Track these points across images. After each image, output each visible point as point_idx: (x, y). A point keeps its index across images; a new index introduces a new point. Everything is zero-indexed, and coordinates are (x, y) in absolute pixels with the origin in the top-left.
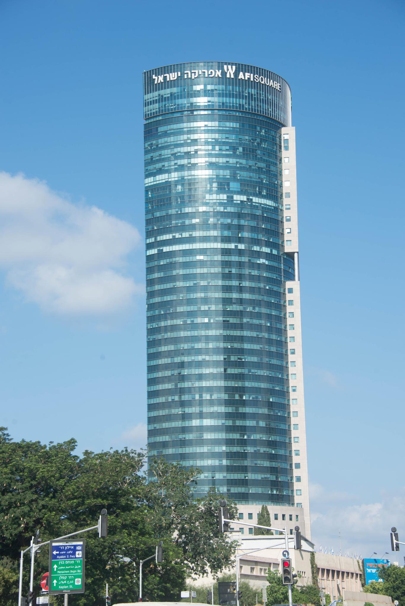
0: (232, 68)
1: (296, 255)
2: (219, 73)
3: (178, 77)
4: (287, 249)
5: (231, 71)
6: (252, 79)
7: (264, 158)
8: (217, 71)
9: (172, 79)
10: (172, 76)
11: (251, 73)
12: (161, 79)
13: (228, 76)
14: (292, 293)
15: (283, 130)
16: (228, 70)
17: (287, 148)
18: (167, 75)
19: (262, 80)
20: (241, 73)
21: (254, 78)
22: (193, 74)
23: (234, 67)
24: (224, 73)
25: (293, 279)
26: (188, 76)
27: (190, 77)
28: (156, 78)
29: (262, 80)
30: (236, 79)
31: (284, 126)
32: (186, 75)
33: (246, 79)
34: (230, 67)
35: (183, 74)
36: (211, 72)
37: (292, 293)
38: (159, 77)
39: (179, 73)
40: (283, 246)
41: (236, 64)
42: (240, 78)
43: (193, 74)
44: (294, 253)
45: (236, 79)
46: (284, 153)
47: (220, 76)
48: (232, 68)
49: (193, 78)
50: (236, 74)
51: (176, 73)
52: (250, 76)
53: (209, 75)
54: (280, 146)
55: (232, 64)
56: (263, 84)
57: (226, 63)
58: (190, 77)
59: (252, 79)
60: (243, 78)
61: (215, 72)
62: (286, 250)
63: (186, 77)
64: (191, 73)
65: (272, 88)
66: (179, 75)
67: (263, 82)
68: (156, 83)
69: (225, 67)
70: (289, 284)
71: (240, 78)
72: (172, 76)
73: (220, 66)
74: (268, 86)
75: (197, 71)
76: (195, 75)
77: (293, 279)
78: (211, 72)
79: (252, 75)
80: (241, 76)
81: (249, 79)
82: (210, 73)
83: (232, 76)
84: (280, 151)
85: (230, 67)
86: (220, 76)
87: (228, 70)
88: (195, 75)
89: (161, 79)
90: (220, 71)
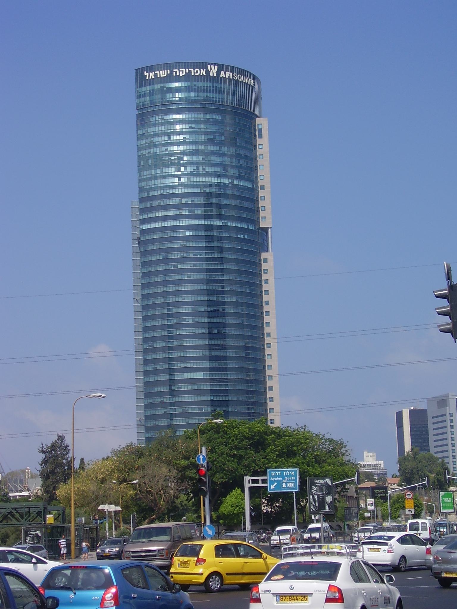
1: (269, 230)
2: (203, 72)
5: (213, 71)
6: (231, 77)
8: (202, 70)
9: (162, 76)
11: (231, 72)
12: (152, 75)
13: (211, 75)
14: (267, 262)
15: (258, 121)
16: (211, 69)
17: (261, 137)
18: (158, 72)
19: (240, 78)
20: (222, 72)
21: (233, 76)
22: (181, 72)
23: (216, 67)
24: (208, 72)
26: (176, 73)
28: (148, 74)
29: (240, 78)
30: (218, 78)
32: (174, 73)
33: (227, 77)
34: (212, 66)
35: (172, 72)
36: (197, 71)
37: (267, 262)
38: (151, 73)
39: (169, 71)
40: (259, 222)
41: (218, 65)
42: (221, 76)
43: (181, 72)
45: (218, 78)
46: (259, 141)
47: (205, 74)
49: (181, 75)
50: (218, 73)
51: (166, 71)
53: (194, 73)
54: (255, 135)
55: (215, 65)
57: (210, 64)
58: (178, 74)
59: (231, 77)
61: (200, 71)
62: (262, 226)
63: (174, 75)
64: (179, 71)
66: (169, 73)
67: (240, 80)
68: (147, 78)
69: (209, 66)
70: (264, 255)
71: (221, 76)
73: (203, 65)
75: (184, 70)
76: (183, 73)
78: (197, 71)
79: (231, 74)
80: (222, 74)
81: (229, 77)
83: (215, 75)
84: (255, 139)
85: (212, 66)
86: (205, 74)
87: (211, 69)
88: (183, 73)
90: (205, 70)
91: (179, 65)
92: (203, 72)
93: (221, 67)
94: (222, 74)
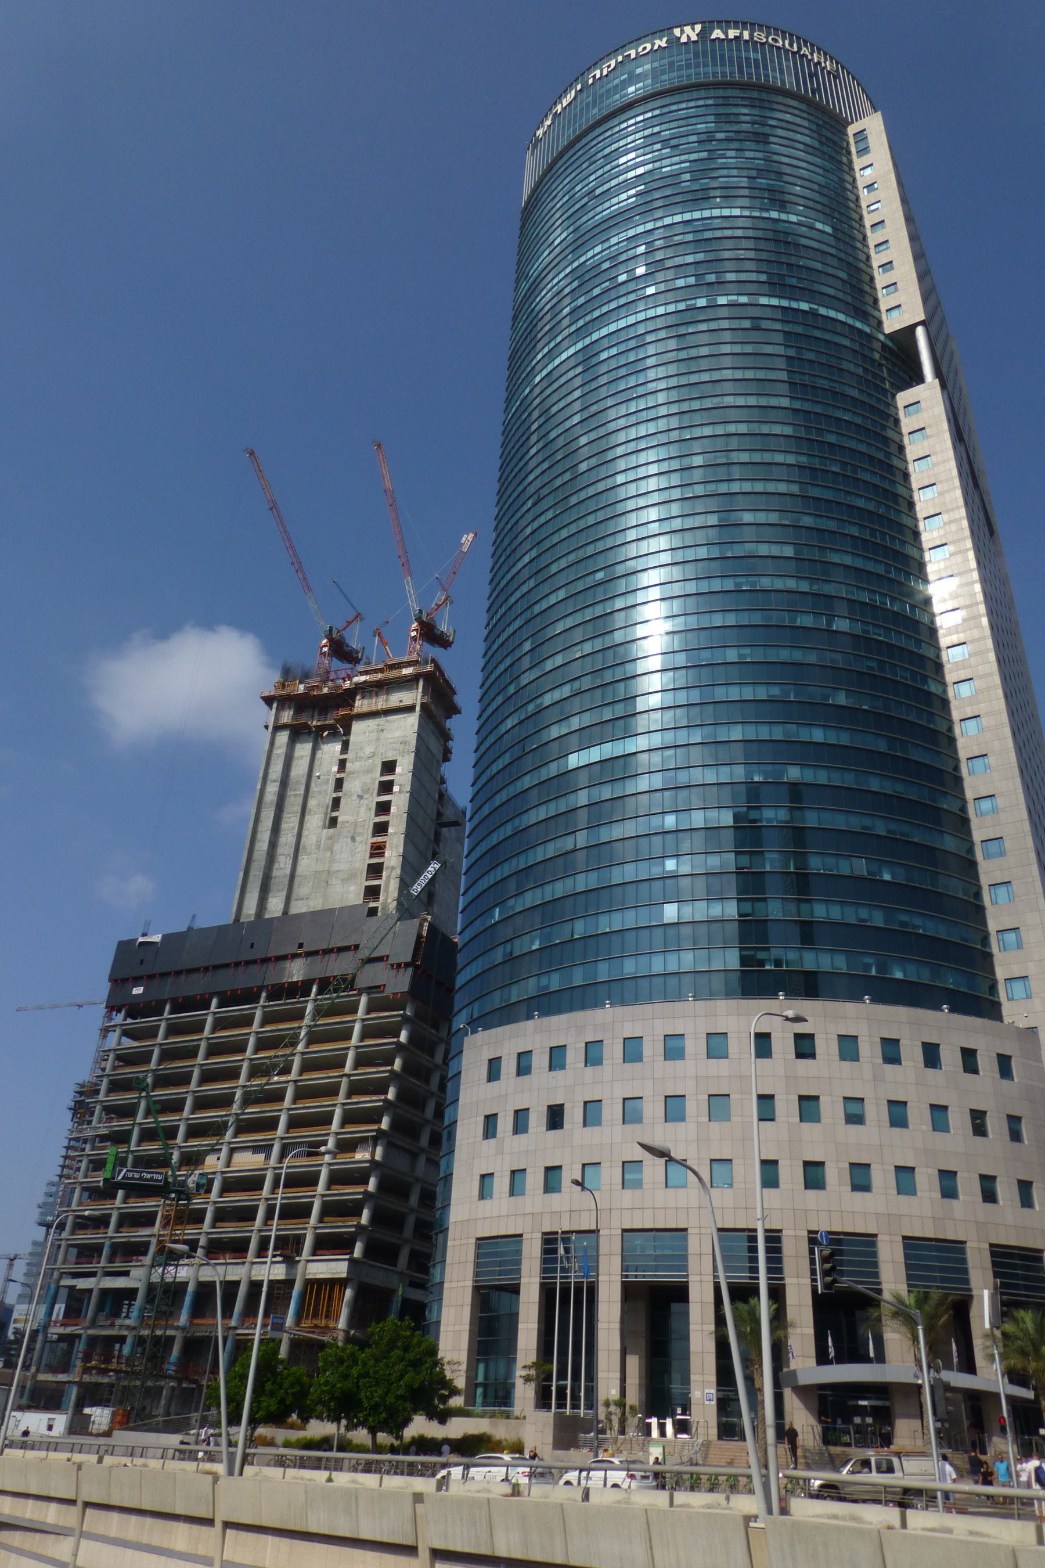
0: (693, 29)
1: (920, 332)
3: (576, 92)
4: (892, 324)
6: (746, 35)
15: (851, 130)
16: (682, 32)
21: (751, 36)
23: (698, 28)
25: (920, 379)
27: (598, 76)
30: (704, 42)
31: (849, 124)
36: (645, 48)
44: (912, 328)
45: (704, 42)
48: (693, 29)
52: (742, 34)
53: (637, 53)
54: (849, 153)
55: (692, 25)
56: (778, 48)
57: (676, 27)
59: (746, 35)
60: (722, 36)
61: (653, 45)
62: (887, 332)
65: (809, 61)
67: (780, 44)
70: (903, 398)
71: (713, 36)
74: (794, 53)
77: (920, 379)
78: (645, 48)
82: (640, 49)
83: (694, 38)
85: (688, 29)
87: (682, 32)
90: (665, 39)
94: (718, 33)
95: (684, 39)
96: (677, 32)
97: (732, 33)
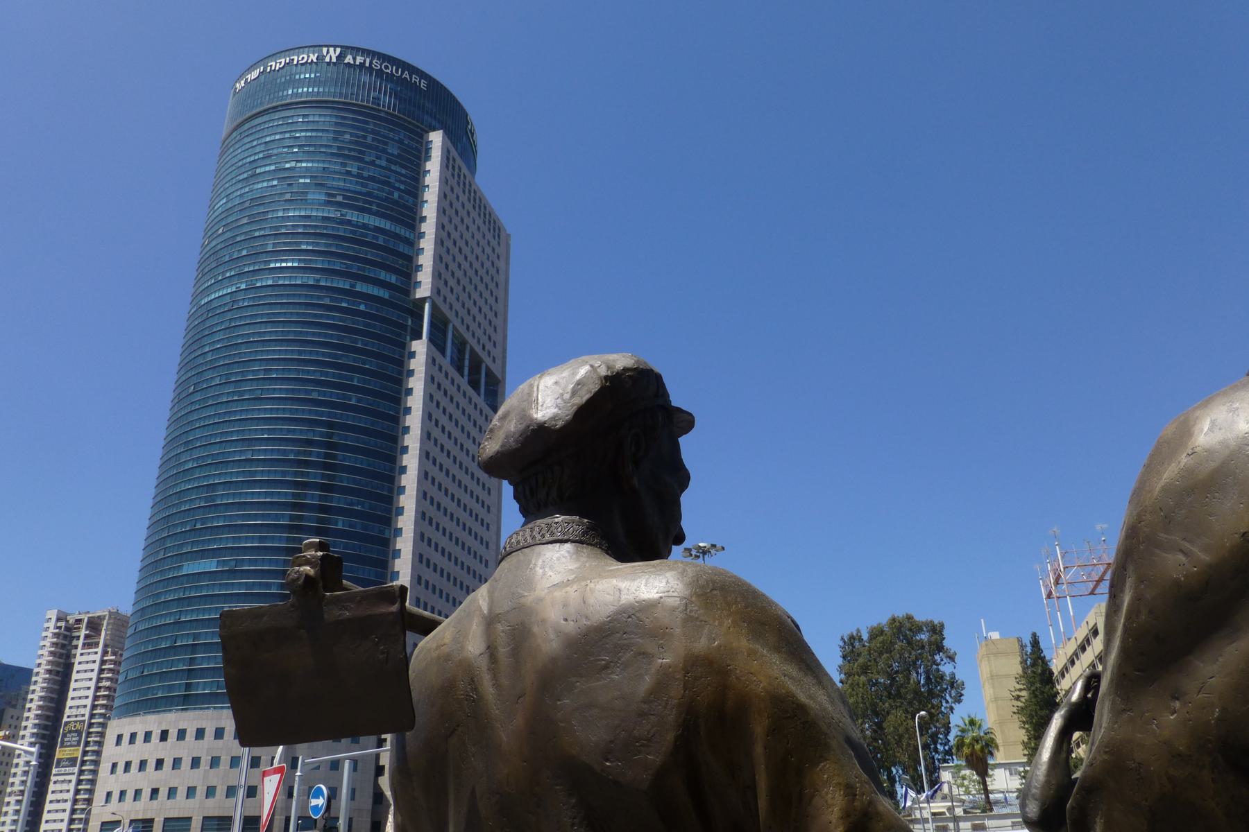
2: (313, 57)
5: (333, 54)
7: (378, 162)
10: (255, 74)
13: (327, 59)
21: (371, 63)
23: (338, 50)
24: (321, 58)
25: (420, 337)
34: (331, 49)
55: (335, 47)
72: (255, 74)
77: (420, 337)
79: (368, 61)
80: (349, 59)
81: (362, 65)
83: (334, 60)
85: (331, 49)
89: (242, 83)
91: (274, 56)
92: (313, 57)
93: (346, 49)
94: (349, 59)
95: (327, 59)
96: (325, 50)
97: (359, 60)
